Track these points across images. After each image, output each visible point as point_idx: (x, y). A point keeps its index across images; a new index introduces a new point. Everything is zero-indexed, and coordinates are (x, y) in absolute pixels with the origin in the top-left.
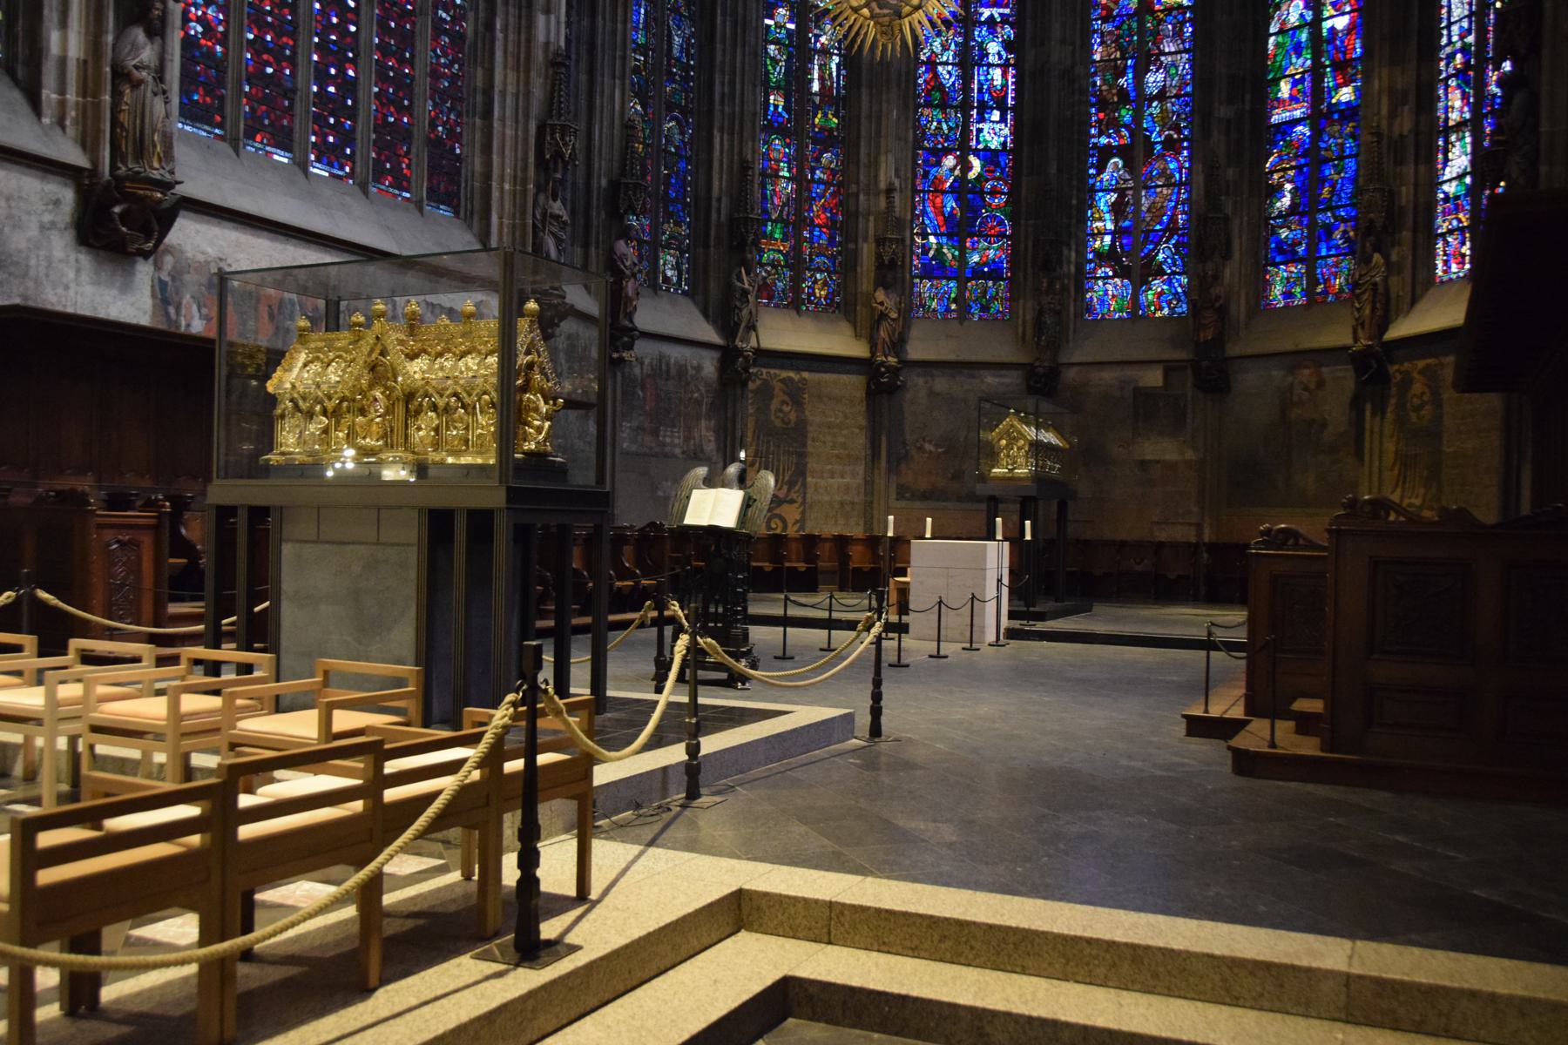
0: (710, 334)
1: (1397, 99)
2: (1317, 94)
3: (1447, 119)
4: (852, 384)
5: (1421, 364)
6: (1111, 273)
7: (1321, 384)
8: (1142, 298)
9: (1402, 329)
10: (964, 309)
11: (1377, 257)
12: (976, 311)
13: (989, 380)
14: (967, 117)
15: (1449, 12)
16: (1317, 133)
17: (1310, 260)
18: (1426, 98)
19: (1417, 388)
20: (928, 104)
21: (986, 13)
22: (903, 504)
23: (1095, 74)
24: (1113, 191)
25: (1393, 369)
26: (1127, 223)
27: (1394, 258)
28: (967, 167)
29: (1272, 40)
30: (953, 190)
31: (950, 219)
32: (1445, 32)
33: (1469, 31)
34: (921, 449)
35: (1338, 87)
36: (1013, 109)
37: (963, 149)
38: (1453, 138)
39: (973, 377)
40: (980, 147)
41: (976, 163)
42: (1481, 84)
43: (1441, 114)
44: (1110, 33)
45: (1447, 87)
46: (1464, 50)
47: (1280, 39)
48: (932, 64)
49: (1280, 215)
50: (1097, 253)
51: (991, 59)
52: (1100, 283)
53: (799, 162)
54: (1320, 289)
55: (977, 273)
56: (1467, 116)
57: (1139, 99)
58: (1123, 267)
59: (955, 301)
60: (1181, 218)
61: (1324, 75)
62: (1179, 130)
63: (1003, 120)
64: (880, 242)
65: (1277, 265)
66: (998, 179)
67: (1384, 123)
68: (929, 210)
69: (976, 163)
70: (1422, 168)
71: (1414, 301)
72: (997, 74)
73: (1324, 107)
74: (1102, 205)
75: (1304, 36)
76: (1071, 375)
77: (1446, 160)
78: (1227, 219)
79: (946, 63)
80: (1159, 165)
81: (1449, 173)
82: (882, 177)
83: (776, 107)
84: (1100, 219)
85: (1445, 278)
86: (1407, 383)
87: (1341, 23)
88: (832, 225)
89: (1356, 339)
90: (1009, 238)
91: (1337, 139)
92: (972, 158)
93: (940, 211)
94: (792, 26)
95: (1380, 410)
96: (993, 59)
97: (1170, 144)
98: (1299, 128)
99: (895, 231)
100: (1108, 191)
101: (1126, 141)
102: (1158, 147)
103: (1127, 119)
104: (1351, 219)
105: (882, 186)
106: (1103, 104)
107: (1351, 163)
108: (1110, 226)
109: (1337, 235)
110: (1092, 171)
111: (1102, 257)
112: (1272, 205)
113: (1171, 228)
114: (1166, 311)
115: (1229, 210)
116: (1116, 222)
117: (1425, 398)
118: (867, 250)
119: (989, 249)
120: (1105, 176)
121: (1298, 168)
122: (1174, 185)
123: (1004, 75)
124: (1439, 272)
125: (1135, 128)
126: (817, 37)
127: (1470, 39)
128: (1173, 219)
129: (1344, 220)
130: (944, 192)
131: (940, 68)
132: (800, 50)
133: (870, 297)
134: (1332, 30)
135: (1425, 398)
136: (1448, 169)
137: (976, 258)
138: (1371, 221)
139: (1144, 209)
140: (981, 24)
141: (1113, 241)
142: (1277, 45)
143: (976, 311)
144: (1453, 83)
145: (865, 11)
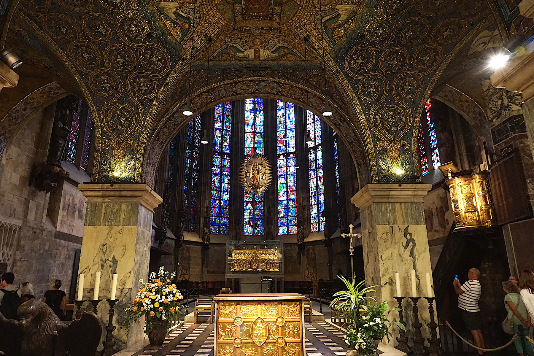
0: (174, 237)
1: (304, 199)
3: (312, 203)
4: (199, 248)
5: (311, 247)
7: (292, 250)
9: (306, 240)
10: (220, 232)
16: (288, 203)
17: (287, 226)
18: (308, 200)
19: (311, 251)
20: (213, 190)
22: (209, 274)
27: (304, 227)
28: (221, 203)
29: (279, 185)
30: (218, 207)
33: (315, 189)
34: (212, 262)
36: (229, 192)
37: (220, 200)
38: (313, 207)
39: (223, 247)
41: (222, 202)
45: (311, 198)
46: (314, 192)
47: (280, 185)
48: (214, 182)
49: (281, 217)
54: (289, 231)
55: (222, 225)
56: (316, 203)
58: (251, 225)
59: (218, 230)
60: (262, 216)
62: (261, 199)
63: (228, 194)
64: (205, 218)
65: (281, 226)
67: (301, 203)
70: (308, 211)
71: (308, 235)
72: (226, 185)
73: (289, 198)
75: (285, 185)
77: (312, 211)
78: (272, 218)
79: (217, 182)
80: (258, 206)
81: (313, 212)
82: (206, 204)
83: (185, 188)
85: (313, 231)
86: (309, 250)
89: (298, 240)
90: (229, 218)
92: (221, 201)
93: (215, 211)
94: (189, 172)
95: (304, 255)
96: (226, 182)
97: (259, 202)
101: (252, 200)
102: (258, 202)
105: (206, 206)
106: (247, 193)
108: (249, 217)
109: (292, 222)
113: (260, 218)
114: (260, 234)
115: (272, 215)
117: (312, 253)
118: (202, 220)
120: (248, 207)
122: (261, 210)
123: (228, 185)
124: (312, 230)
126: (193, 175)
127: (316, 191)
129: (294, 219)
130: (216, 208)
131: (216, 183)
132: (190, 176)
135: (312, 253)
137: (222, 222)
138: (301, 220)
140: (224, 175)
141: (249, 220)
142: (280, 186)
144: (313, 197)
145: (251, 187)
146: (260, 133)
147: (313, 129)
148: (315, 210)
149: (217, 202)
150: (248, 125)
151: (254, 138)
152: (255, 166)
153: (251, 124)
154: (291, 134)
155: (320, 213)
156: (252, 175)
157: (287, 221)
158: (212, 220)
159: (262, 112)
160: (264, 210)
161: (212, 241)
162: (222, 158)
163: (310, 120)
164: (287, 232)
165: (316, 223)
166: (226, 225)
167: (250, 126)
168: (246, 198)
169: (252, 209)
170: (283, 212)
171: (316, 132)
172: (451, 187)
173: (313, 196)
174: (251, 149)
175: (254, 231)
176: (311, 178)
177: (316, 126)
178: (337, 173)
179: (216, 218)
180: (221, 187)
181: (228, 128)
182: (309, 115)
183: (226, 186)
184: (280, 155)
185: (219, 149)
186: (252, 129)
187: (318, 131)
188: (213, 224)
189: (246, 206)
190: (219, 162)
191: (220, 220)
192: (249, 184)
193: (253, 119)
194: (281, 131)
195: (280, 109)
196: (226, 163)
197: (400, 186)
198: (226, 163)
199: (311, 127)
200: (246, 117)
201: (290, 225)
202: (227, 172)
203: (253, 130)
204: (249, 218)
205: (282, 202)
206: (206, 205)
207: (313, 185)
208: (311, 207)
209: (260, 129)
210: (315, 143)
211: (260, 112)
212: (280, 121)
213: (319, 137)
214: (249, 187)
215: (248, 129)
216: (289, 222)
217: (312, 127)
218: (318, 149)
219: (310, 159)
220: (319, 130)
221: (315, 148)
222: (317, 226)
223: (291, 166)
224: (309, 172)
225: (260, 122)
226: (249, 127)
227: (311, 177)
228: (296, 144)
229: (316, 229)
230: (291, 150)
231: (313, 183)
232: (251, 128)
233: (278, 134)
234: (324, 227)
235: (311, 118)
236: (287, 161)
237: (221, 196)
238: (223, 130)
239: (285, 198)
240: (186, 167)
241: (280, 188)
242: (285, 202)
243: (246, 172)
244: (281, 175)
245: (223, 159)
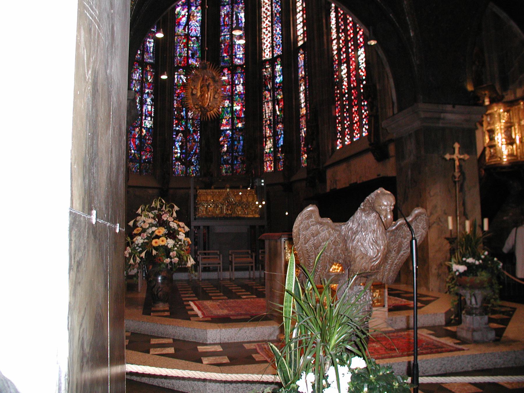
2: (233, 124)
3: (266, 135)
6: (180, 164)
8: (188, 171)
10: (141, 172)
12: (144, 171)
14: (142, 118)
15: (265, 111)
17: (232, 164)
21: (147, 91)
23: (175, 111)
24: (181, 142)
26: (184, 151)
28: (142, 132)
32: (264, 115)
33: (271, 116)
35: (238, 123)
36: (153, 117)
38: (268, 139)
40: (145, 126)
41: (144, 131)
43: (264, 133)
44: (179, 101)
45: (265, 128)
46: (270, 120)
47: (223, 109)
51: (148, 103)
52: (177, 166)
54: (235, 172)
56: (271, 135)
57: (187, 119)
59: (139, 169)
61: (234, 120)
63: (151, 120)
66: (150, 136)
68: (132, 143)
69: (144, 131)
72: (149, 107)
73: (234, 128)
74: (177, 145)
76: (171, 191)
77: (266, 144)
84: (177, 149)
87: (238, 108)
90: (153, 152)
93: (134, 143)
97: (194, 131)
98: (228, 132)
100: (178, 142)
102: (192, 132)
103: (184, 123)
104: (243, 155)
106: (177, 119)
107: (242, 142)
108: (179, 151)
110: (174, 136)
111: (178, 159)
112: (222, 150)
113: (195, 153)
116: (181, 150)
119: (147, 155)
120: (178, 138)
121: (229, 142)
125: (186, 127)
127: (271, 118)
128: (196, 151)
129: (240, 155)
134: (236, 109)
136: (266, 147)
137: (144, 157)
139: (188, 147)
140: (146, 93)
141: (180, 155)
142: (222, 111)
143: (144, 171)
144: (267, 127)
145: (199, 109)
147: (270, 35)
148: (269, 145)
149: (137, 130)
150: (179, 25)
151: (187, 43)
152: (205, 81)
153: (184, 24)
155: (277, 147)
156: (201, 92)
157: (232, 158)
158: (131, 155)
159: (199, 7)
162: (142, 70)
163: (267, 22)
165: (271, 161)
167: (183, 27)
168: (176, 127)
169: (185, 141)
170: (226, 146)
171: (275, 39)
172: (487, 115)
173: (268, 125)
174: (184, 59)
176: (264, 101)
177: (274, 32)
178: (302, 96)
179: (136, 152)
180: (142, 110)
182: (265, 16)
183: (148, 108)
184: (223, 68)
185: (139, 56)
186: (185, 31)
187: (277, 39)
189: (176, 137)
190: (139, 75)
191: (141, 155)
192: (197, 105)
193: (186, 16)
194: (225, 35)
195: (224, 6)
196: (149, 77)
197: (454, 107)
198: (149, 77)
199: (267, 32)
200: (176, 12)
201: (236, 162)
202: (148, 88)
203: (186, 33)
204: (180, 153)
205: (224, 132)
207: (267, 112)
208: (264, 140)
209: (195, 31)
210: (273, 54)
212: (224, 23)
213: (278, 47)
214: (196, 109)
215: (180, 30)
217: (269, 32)
218: (277, 62)
219: (265, 76)
220: (278, 38)
221: (273, 62)
222: (272, 165)
223: (238, 85)
224: (262, 92)
225: (197, 21)
227: (266, 100)
228: (246, 54)
229: (271, 168)
230: (238, 62)
231: (268, 108)
232: (184, 29)
233: (221, 40)
234: (284, 165)
235: (267, 21)
241: (223, 114)
243: (191, 88)
245: (144, 72)
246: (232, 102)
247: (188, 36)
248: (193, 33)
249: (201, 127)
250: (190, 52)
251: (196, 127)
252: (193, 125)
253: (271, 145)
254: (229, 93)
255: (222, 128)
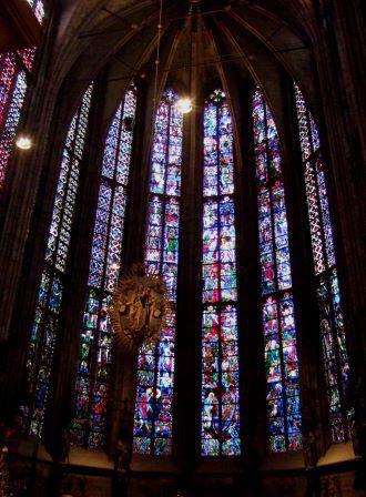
2: (283, 373)
5: (332, 476)
10: (153, 449)
11: (310, 434)
13: (164, 481)
14: (156, 375)
17: (286, 434)
19: (332, 486)
25: (321, 478)
28: (155, 393)
31: (148, 414)
37: (155, 387)
42: (339, 372)
46: (332, 360)
48: (143, 355)
50: (207, 431)
53: (90, 388)
57: (221, 372)
71: (325, 452)
72: (167, 360)
80: (227, 396)
86: (327, 484)
88: (102, 414)
91: (293, 390)
97: (231, 388)
99: (129, 415)
105: (123, 399)
106: (207, 373)
107: (297, 399)
108: (210, 419)
113: (233, 421)
120: (208, 399)
121: (279, 399)
125: (220, 383)
133: (116, 443)
146: (231, 263)
148: (335, 399)
150: (208, 251)
151: (219, 272)
154: (283, 258)
159: (232, 227)
160: (241, 402)
161: (134, 467)
163: (316, 225)
164: (286, 446)
166: (166, 436)
175: (220, 447)
180: (156, 365)
181: (170, 258)
183: (167, 360)
184: (267, 297)
188: (139, 434)
195: (263, 219)
206: (125, 395)
210: (327, 266)
211: (229, 226)
215: (208, 258)
216: (287, 424)
221: (327, 274)
226: (210, 254)
228: (292, 274)
232: (214, 256)
236: (278, 309)
237: (156, 380)
238: (162, 262)
239: (277, 379)
240: (88, 329)
242: (279, 386)
244: (270, 335)
246: (280, 341)
247: (219, 264)
248: (225, 259)
249: (240, 382)
250: (222, 283)
251: (233, 382)
252: (229, 379)
253: (337, 399)
254: (276, 330)
255: (269, 381)
